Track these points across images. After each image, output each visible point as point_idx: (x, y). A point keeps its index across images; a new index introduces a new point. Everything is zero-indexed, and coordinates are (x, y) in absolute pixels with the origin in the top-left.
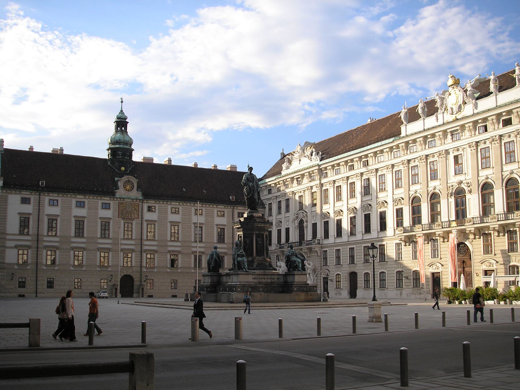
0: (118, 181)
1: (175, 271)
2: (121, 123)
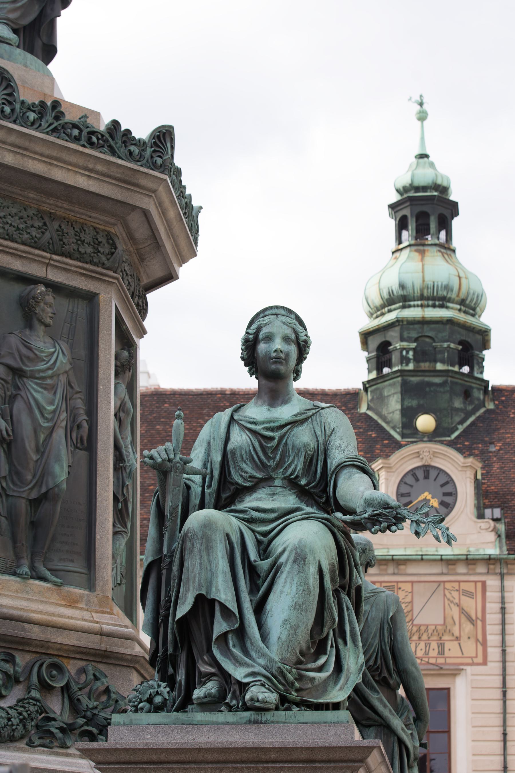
2: (426, 213)
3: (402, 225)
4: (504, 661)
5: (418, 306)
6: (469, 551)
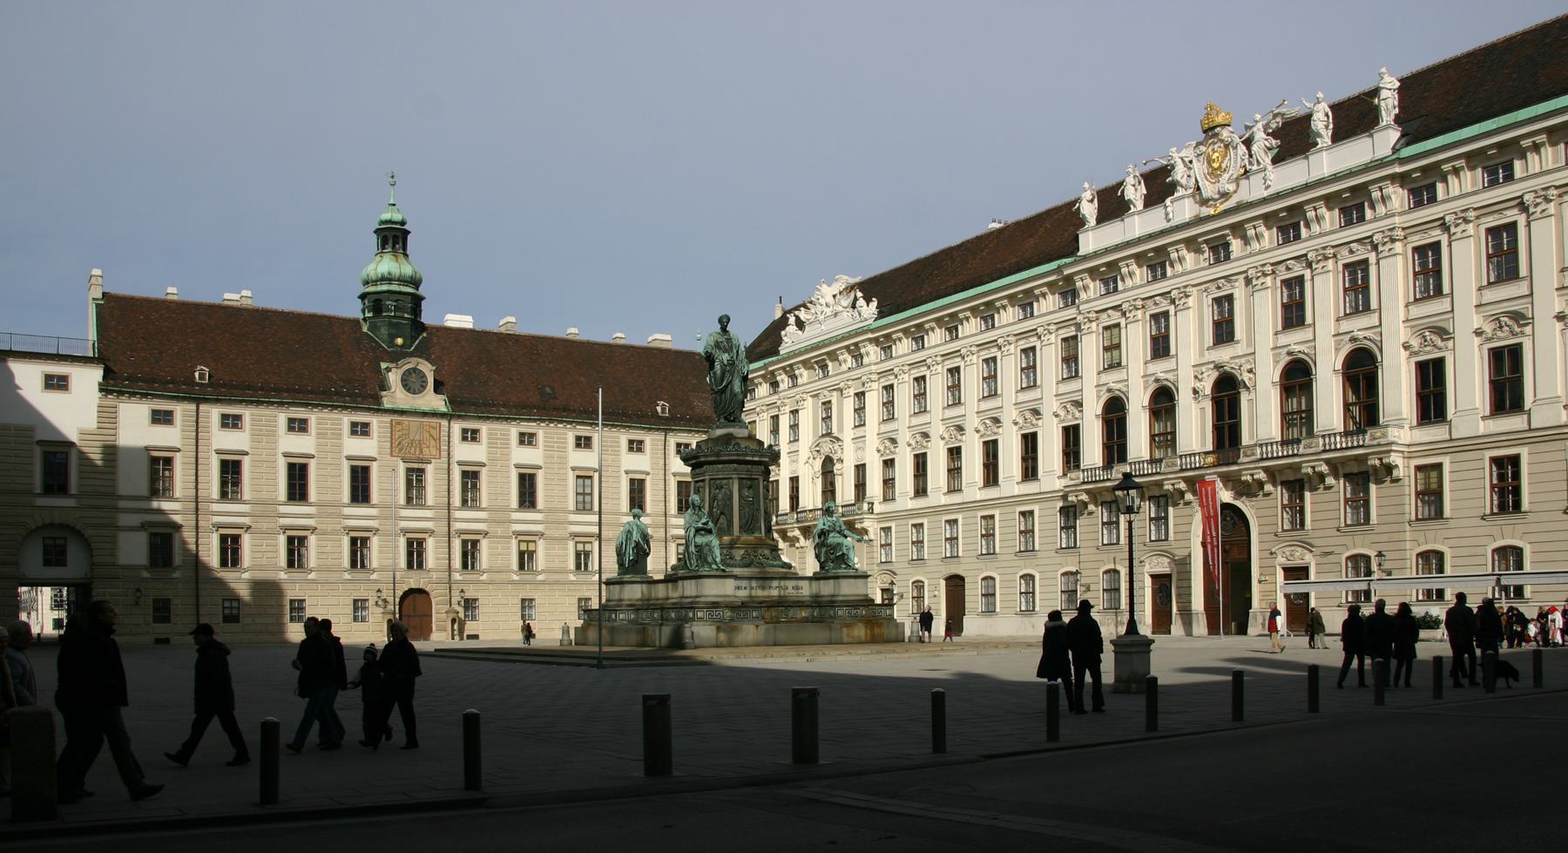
0: (388, 370)
1: (528, 577)
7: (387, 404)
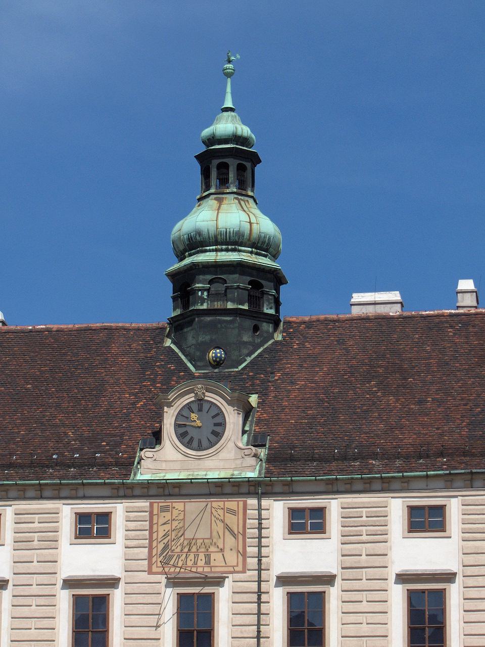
3: (206, 174)
4: (260, 570)
5: (213, 250)
6: (233, 475)
7: (143, 475)
